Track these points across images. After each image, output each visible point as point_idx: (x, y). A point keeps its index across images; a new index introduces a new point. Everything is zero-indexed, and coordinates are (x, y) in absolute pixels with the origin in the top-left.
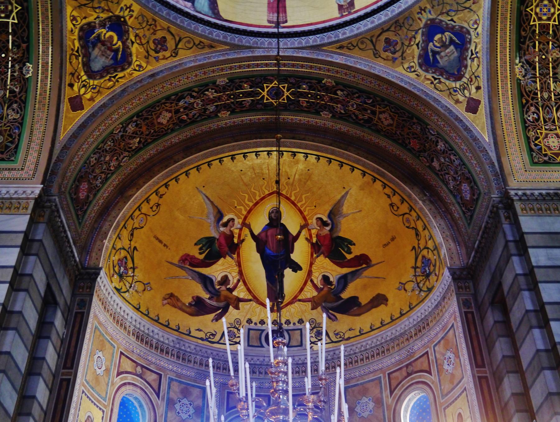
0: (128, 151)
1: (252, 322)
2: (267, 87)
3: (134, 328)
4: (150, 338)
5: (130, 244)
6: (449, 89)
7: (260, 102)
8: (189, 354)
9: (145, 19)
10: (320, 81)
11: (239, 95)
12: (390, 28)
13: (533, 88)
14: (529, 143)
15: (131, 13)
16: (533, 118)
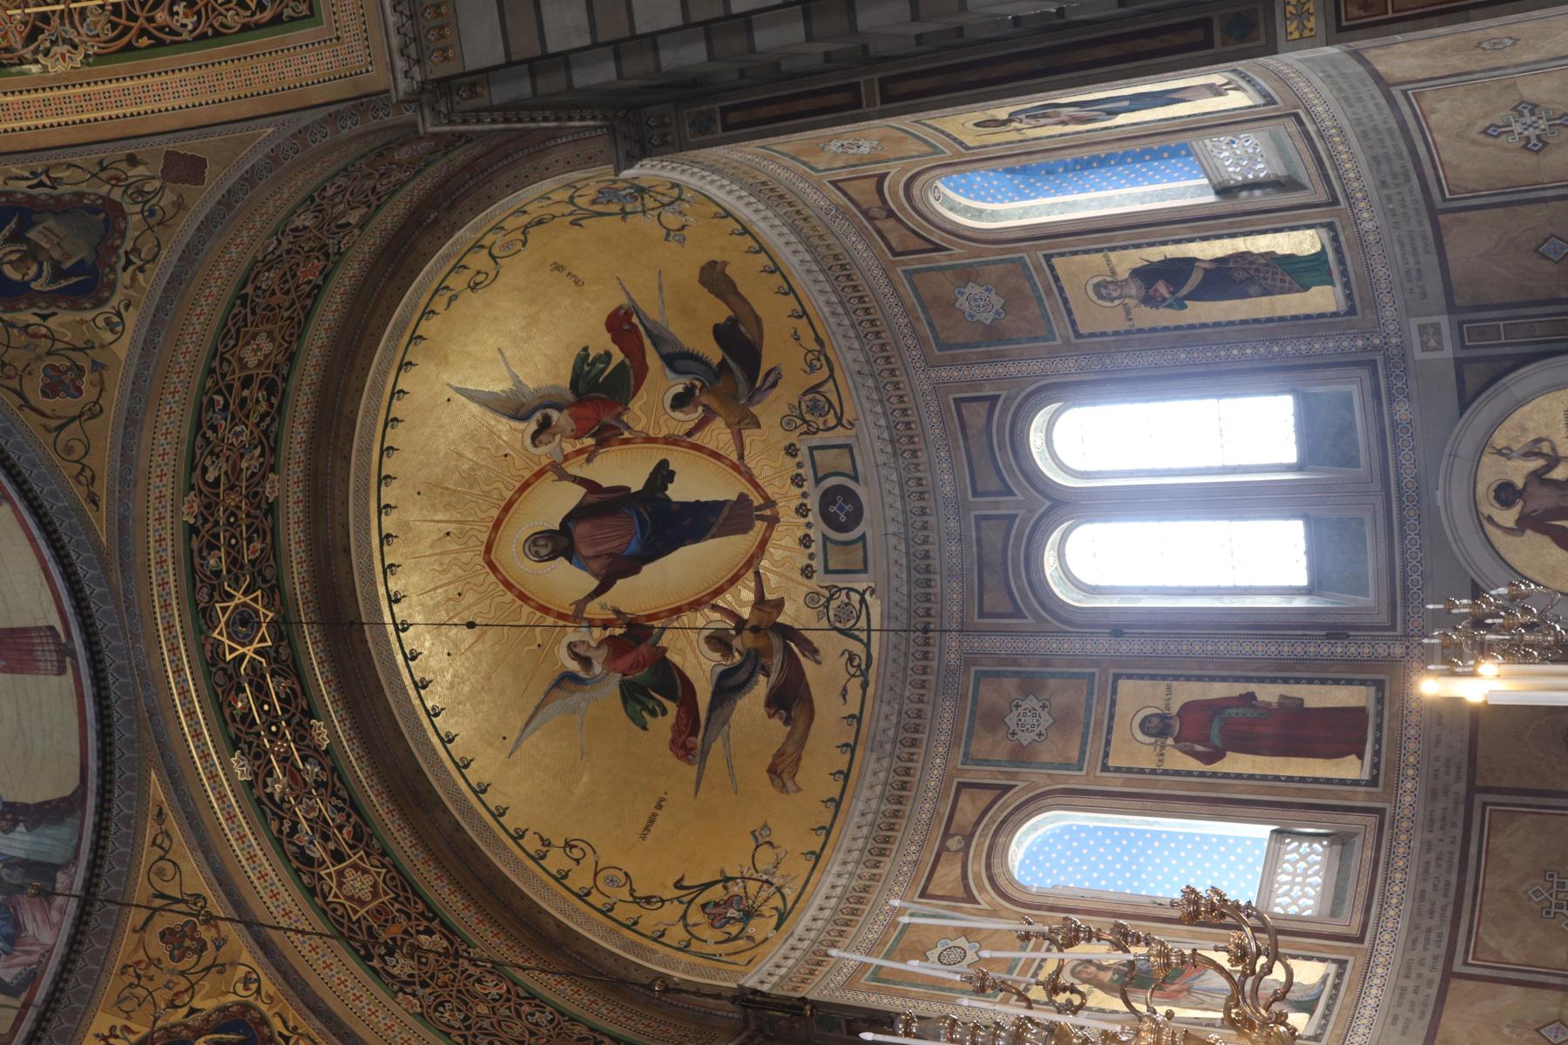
2: (232, 650)
3: (861, 866)
4: (879, 821)
5: (671, 900)
6: (150, 228)
7: (273, 654)
8: (904, 716)
9: (126, 993)
10: (192, 530)
11: (267, 713)
12: (15, 391)
13: (103, 19)
14: (258, 26)
15: (118, 1032)
16: (186, 16)
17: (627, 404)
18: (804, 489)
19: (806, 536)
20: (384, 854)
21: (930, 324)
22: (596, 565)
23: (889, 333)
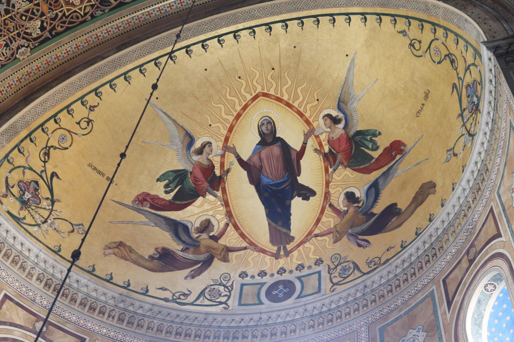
0: (24, 38)
1: (247, 275)
5: (45, 167)
17: (348, 167)
18: (295, 271)
19: (266, 274)
20: (93, 16)
21: (397, 319)
22: (256, 159)
23: (391, 297)
